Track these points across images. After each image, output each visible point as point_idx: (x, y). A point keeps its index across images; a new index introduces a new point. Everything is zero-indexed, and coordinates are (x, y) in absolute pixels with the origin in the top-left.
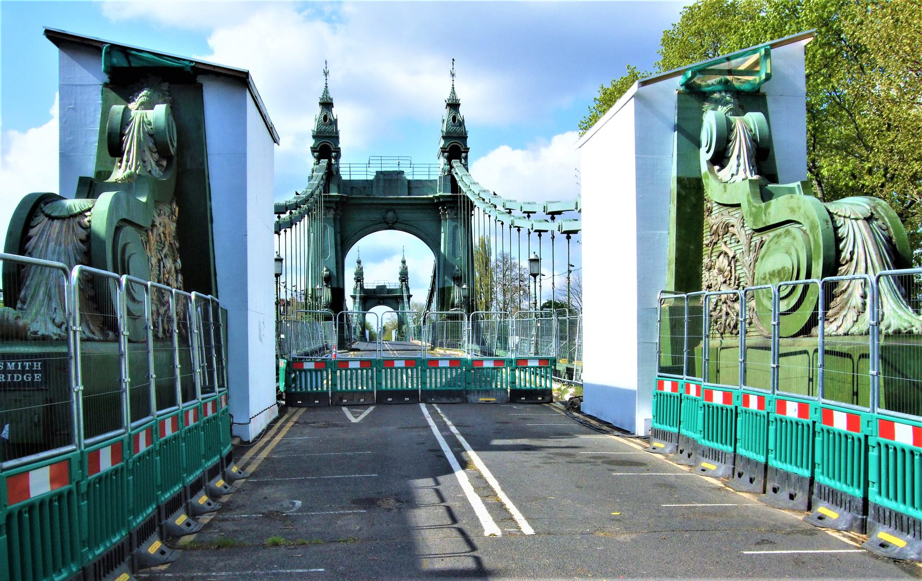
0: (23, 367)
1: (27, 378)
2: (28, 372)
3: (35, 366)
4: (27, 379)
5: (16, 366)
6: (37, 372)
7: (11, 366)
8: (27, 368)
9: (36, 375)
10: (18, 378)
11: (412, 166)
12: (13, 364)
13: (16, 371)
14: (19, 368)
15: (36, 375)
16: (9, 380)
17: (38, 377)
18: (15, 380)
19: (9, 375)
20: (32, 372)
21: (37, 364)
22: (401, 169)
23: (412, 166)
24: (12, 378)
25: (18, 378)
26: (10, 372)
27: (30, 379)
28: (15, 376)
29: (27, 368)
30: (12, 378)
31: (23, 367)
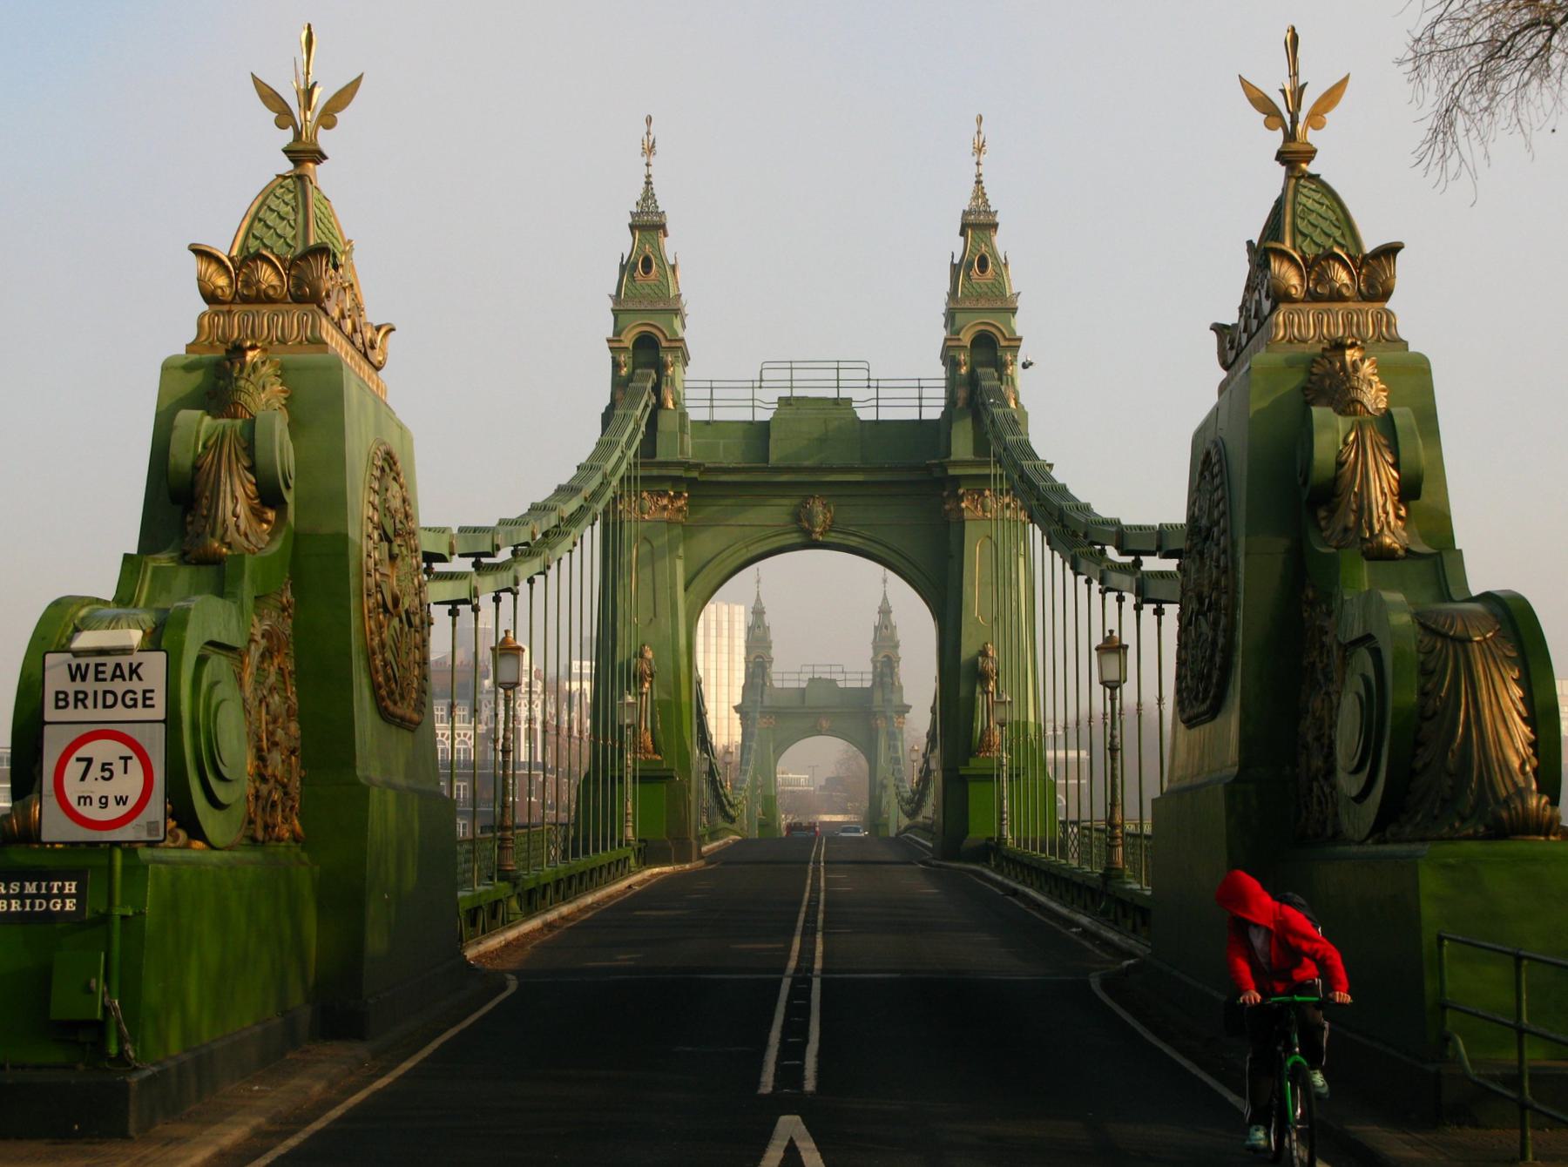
0: (49, 888)
2: (56, 896)
3: (67, 887)
5: (39, 888)
6: (70, 896)
7: (31, 888)
8: (55, 891)
9: (68, 901)
11: (873, 384)
12: (34, 884)
13: (38, 896)
14: (43, 891)
15: (68, 901)
16: (28, 909)
17: (70, 905)
18: (37, 909)
19: (28, 902)
20: (62, 896)
21: (70, 890)
22: (844, 394)
23: (873, 384)
24: (32, 905)
25: (41, 905)
27: (58, 907)
28: (37, 902)
29: (55, 891)
30: (32, 905)
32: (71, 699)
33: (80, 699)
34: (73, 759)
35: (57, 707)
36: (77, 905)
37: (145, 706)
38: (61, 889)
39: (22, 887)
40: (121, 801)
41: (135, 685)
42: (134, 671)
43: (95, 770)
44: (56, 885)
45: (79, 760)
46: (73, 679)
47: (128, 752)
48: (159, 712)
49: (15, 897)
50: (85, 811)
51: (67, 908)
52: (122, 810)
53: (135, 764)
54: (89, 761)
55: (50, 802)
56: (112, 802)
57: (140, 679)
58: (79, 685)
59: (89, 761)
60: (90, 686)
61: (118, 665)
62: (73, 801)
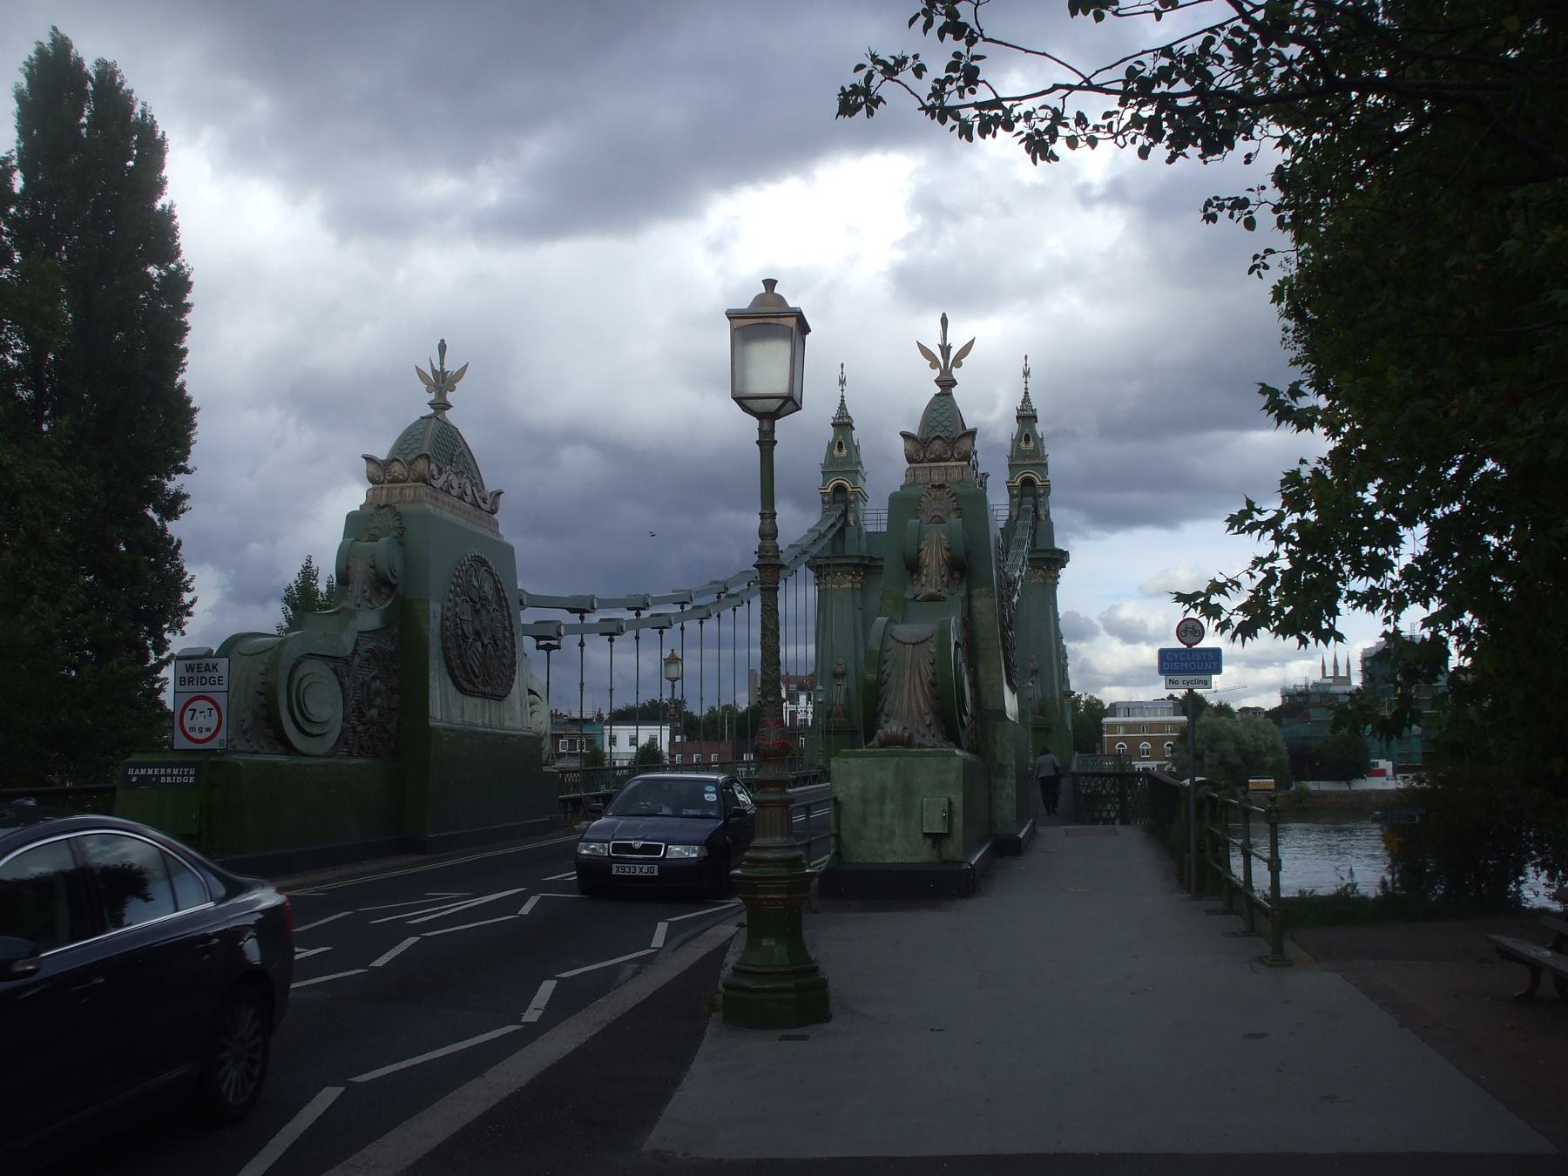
0: (183, 772)
5: (179, 771)
6: (191, 775)
7: (175, 772)
13: (178, 775)
24: (176, 780)
26: (175, 775)
30: (176, 780)
31: (183, 772)
32: (187, 681)
33: (191, 681)
34: (187, 711)
35: (181, 685)
37: (219, 684)
39: (172, 771)
40: (208, 730)
41: (216, 675)
42: (214, 667)
43: (197, 714)
44: (186, 770)
45: (190, 710)
46: (188, 671)
47: (211, 706)
48: (224, 688)
50: (191, 734)
52: (209, 734)
53: (214, 712)
54: (194, 710)
55: (178, 731)
56: (204, 730)
57: (217, 671)
58: (190, 674)
59: (194, 710)
60: (195, 674)
61: (208, 665)
62: (187, 730)
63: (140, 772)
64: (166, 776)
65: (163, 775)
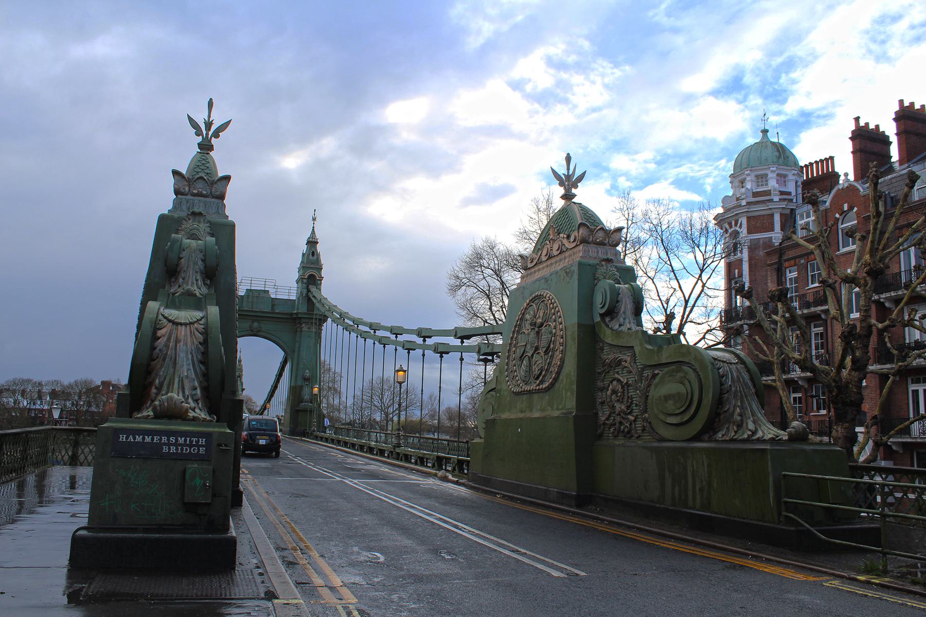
0: (191, 441)
1: (194, 450)
2: (195, 446)
3: (200, 441)
4: (194, 451)
5: (185, 440)
6: (202, 446)
7: (181, 440)
8: (194, 443)
10: (186, 450)
13: (185, 444)
16: (179, 451)
18: (184, 452)
24: (182, 449)
25: (187, 450)
28: (185, 448)
30: (182, 449)
31: (191, 441)
36: (206, 451)
38: (197, 442)
49: (172, 445)
51: (201, 452)
63: (135, 438)
64: (169, 444)
65: (165, 444)
